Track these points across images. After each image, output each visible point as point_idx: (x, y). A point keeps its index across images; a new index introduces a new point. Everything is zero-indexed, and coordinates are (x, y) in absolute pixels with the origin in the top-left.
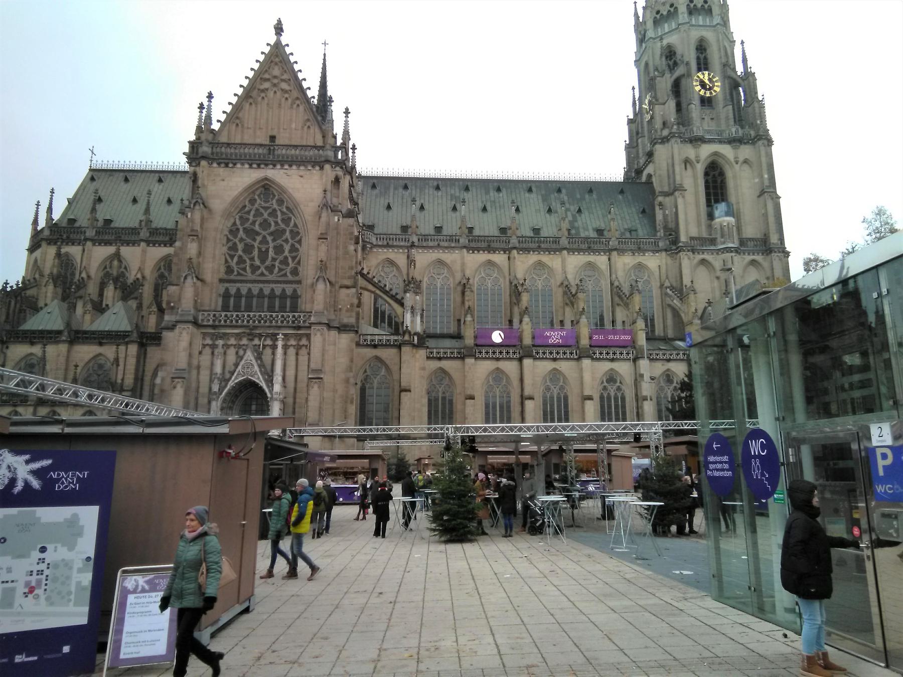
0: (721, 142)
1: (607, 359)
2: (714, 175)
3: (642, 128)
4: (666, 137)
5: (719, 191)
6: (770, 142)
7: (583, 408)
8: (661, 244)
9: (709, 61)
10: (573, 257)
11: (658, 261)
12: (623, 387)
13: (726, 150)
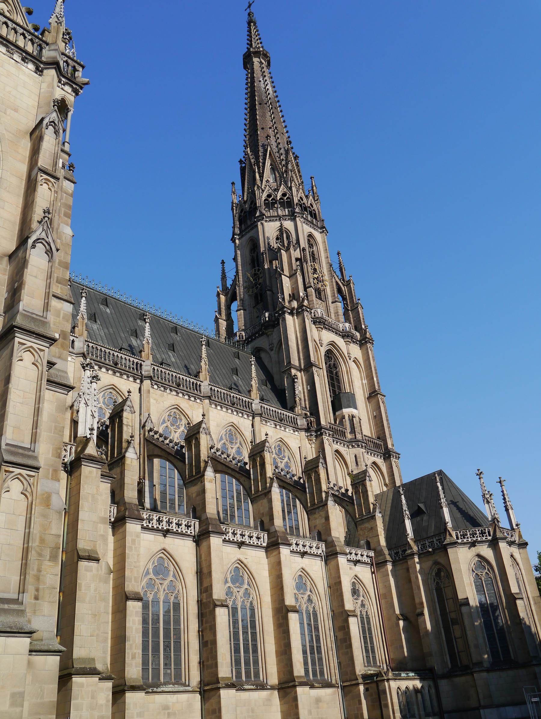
8: (299, 422)
11: (298, 441)
12: (314, 598)
13: (340, 342)
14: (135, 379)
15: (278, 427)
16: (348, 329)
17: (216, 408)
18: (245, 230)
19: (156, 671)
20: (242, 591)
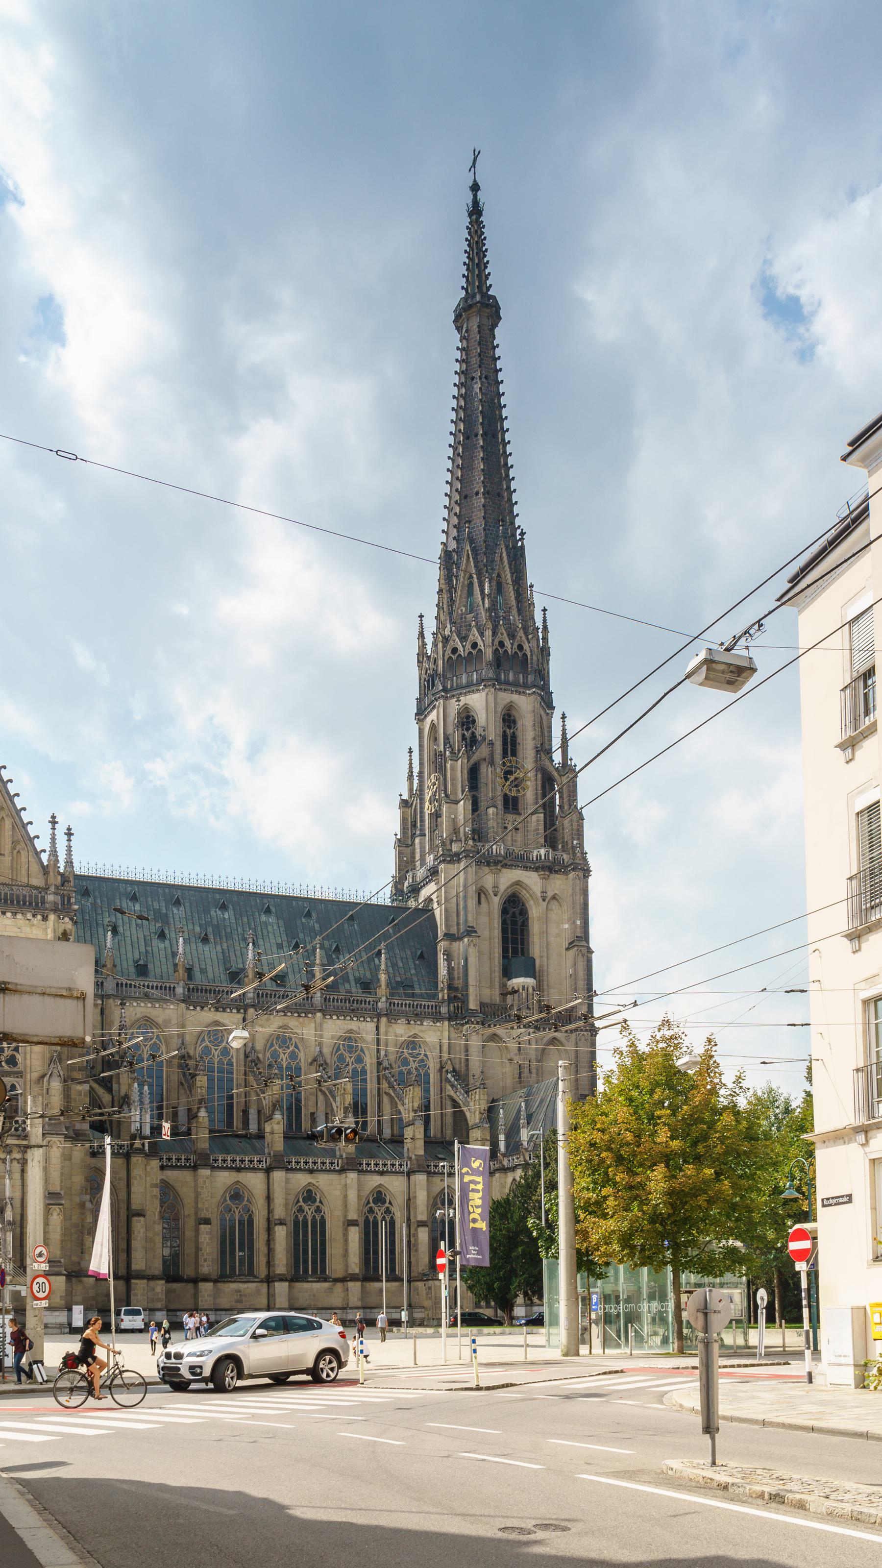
0: (526, 868)
1: (375, 1172)
2: (514, 913)
3: (422, 821)
4: (457, 854)
5: (519, 937)
6: (586, 872)
7: (345, 1235)
8: (444, 1010)
9: (519, 740)
10: (330, 1022)
12: (393, 1209)
13: (532, 880)
14: (238, 1011)
15: (412, 1022)
16: (543, 857)
17: (331, 1018)
18: (429, 705)
19: (233, 1267)
20: (313, 1208)
